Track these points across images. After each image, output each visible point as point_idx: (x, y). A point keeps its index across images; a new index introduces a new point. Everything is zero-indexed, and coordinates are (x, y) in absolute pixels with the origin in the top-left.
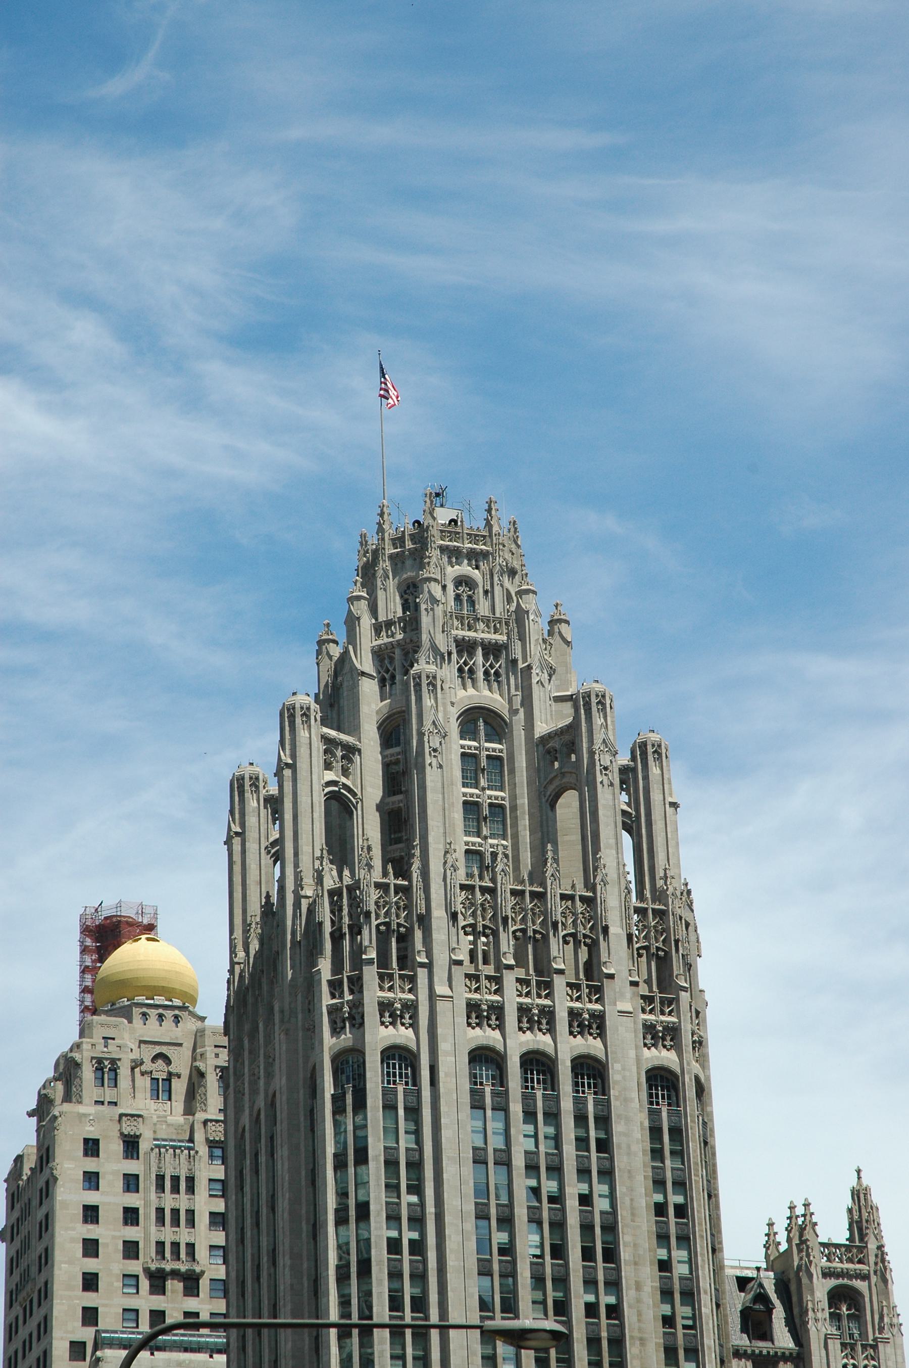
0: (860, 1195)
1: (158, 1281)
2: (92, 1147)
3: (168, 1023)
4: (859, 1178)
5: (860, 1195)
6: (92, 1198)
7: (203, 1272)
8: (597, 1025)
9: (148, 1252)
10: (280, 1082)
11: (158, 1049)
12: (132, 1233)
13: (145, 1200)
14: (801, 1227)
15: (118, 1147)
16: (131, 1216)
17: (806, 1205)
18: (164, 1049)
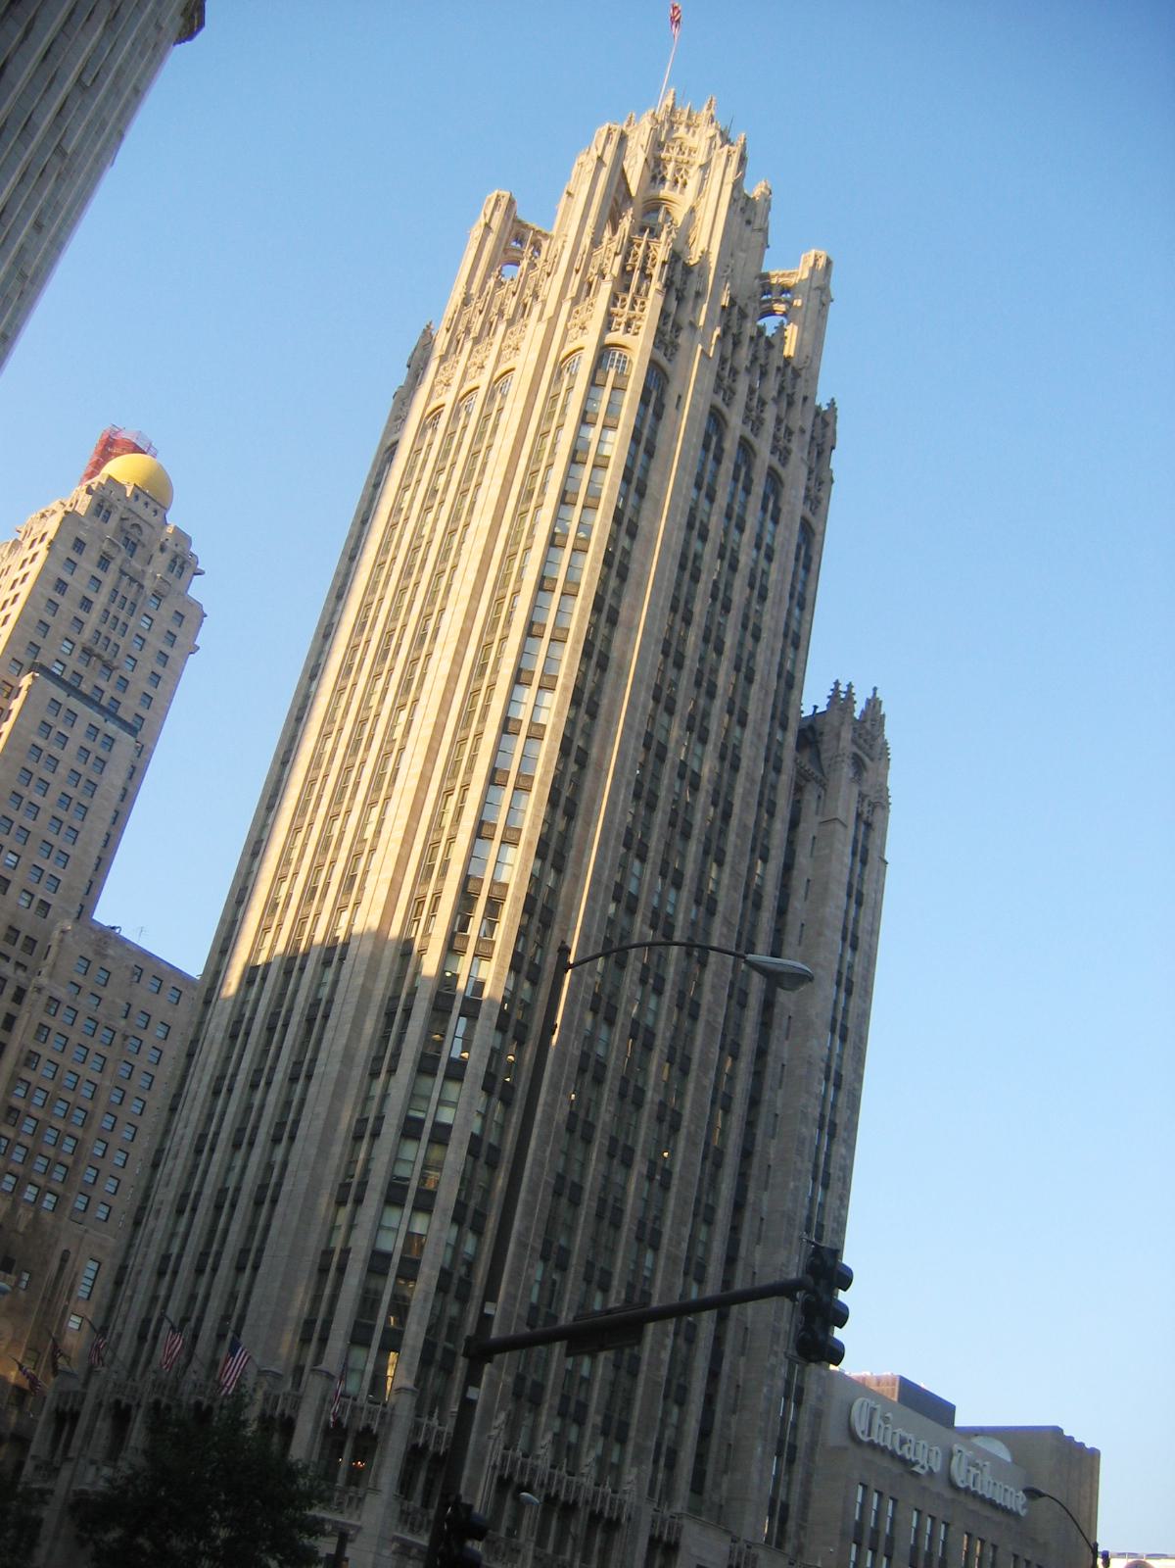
0: (874, 704)
1: (87, 652)
2: (79, 545)
3: (149, 511)
4: (875, 694)
5: (874, 704)
6: (66, 578)
7: (117, 668)
8: (784, 455)
9: (88, 632)
10: (524, 363)
11: (137, 521)
12: (82, 614)
13: (100, 600)
14: (841, 700)
15: (95, 556)
16: (86, 604)
17: (850, 686)
18: (142, 524)
